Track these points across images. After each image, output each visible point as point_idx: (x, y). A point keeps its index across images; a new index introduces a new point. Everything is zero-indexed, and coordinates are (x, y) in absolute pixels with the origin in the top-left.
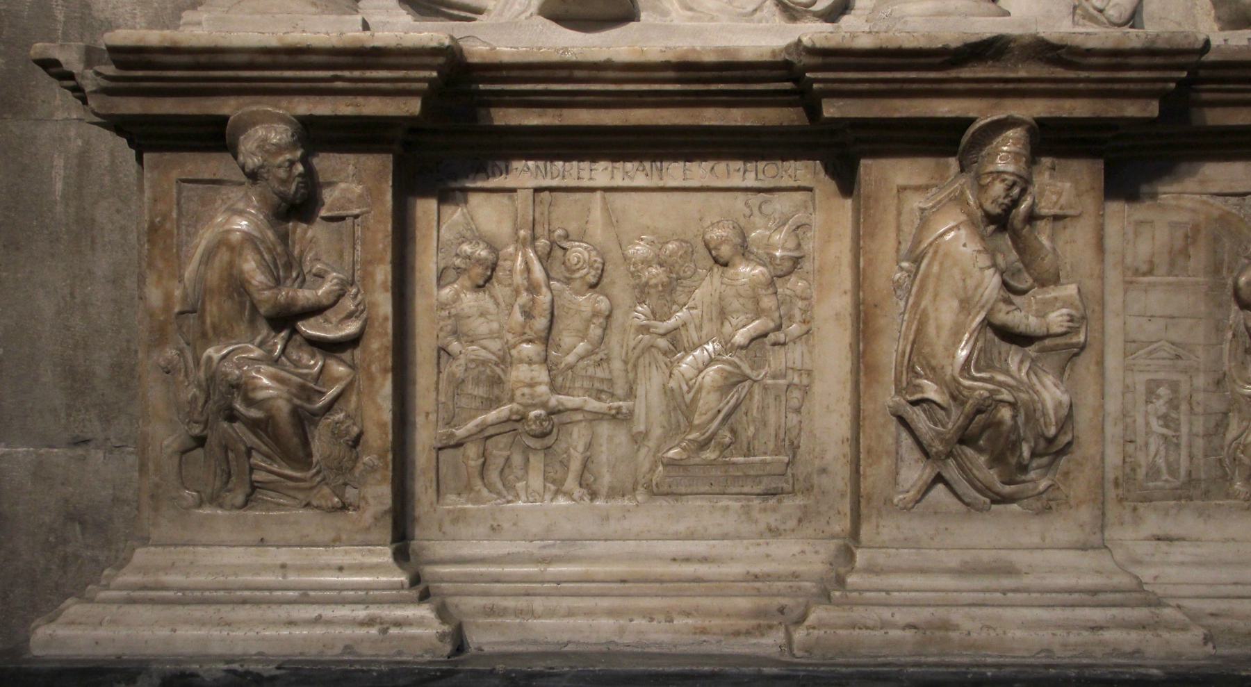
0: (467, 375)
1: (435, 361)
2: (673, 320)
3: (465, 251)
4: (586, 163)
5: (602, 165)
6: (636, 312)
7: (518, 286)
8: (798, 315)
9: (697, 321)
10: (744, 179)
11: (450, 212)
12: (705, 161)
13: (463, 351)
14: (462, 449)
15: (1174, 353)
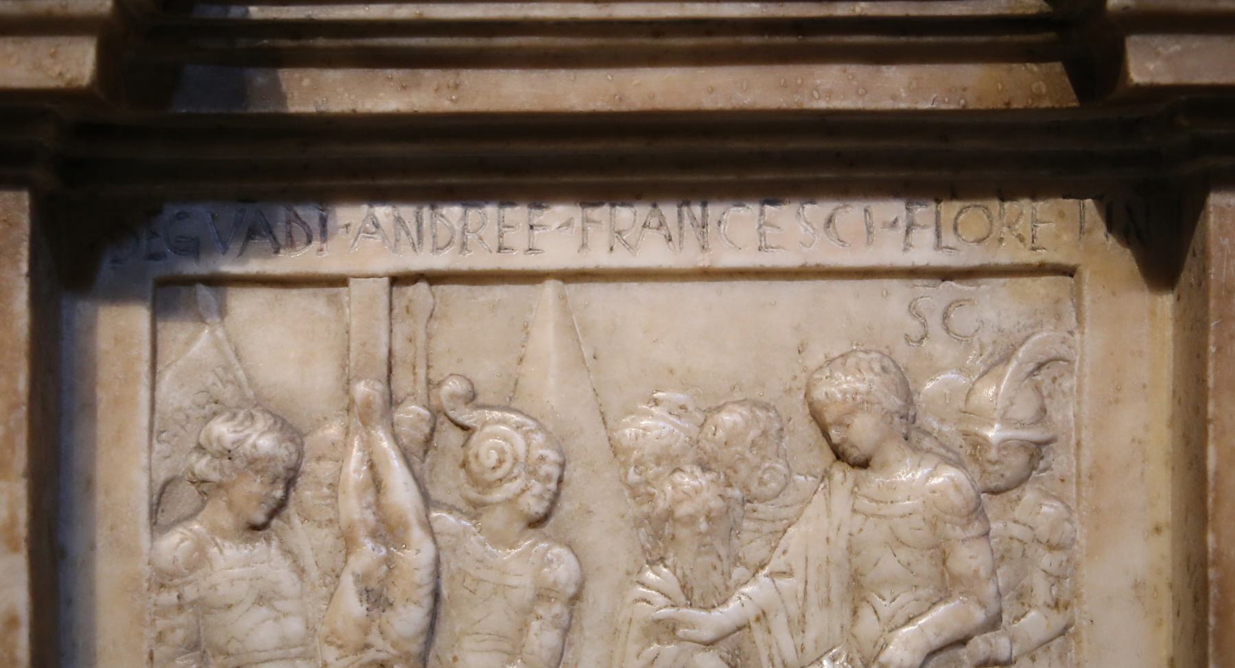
2: (733, 605)
3: (219, 440)
4: (517, 208)
5: (559, 213)
6: (643, 585)
7: (351, 527)
8: (1042, 590)
9: (794, 609)
10: (907, 247)
11: (182, 336)
12: (812, 202)
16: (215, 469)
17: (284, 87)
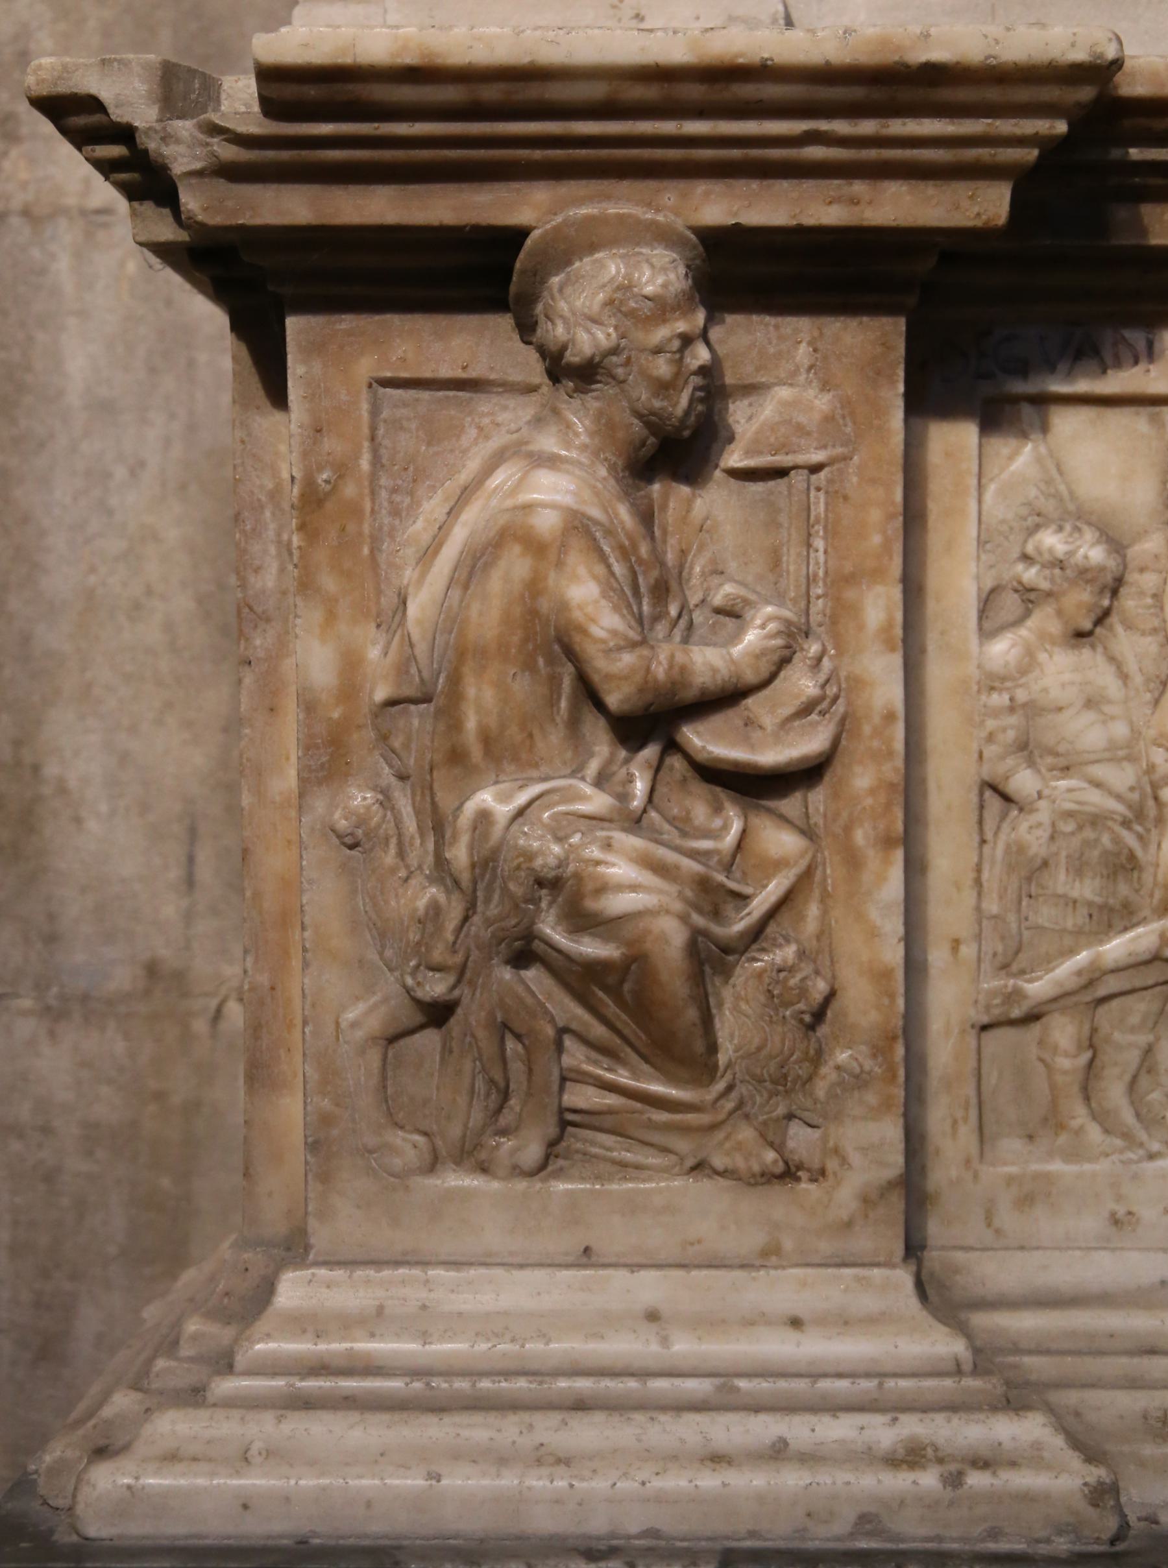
0: (1054, 849)
1: (974, 817)
13: (1046, 792)
14: (1036, 1029)
16: (1045, 578)
17: (1146, 221)
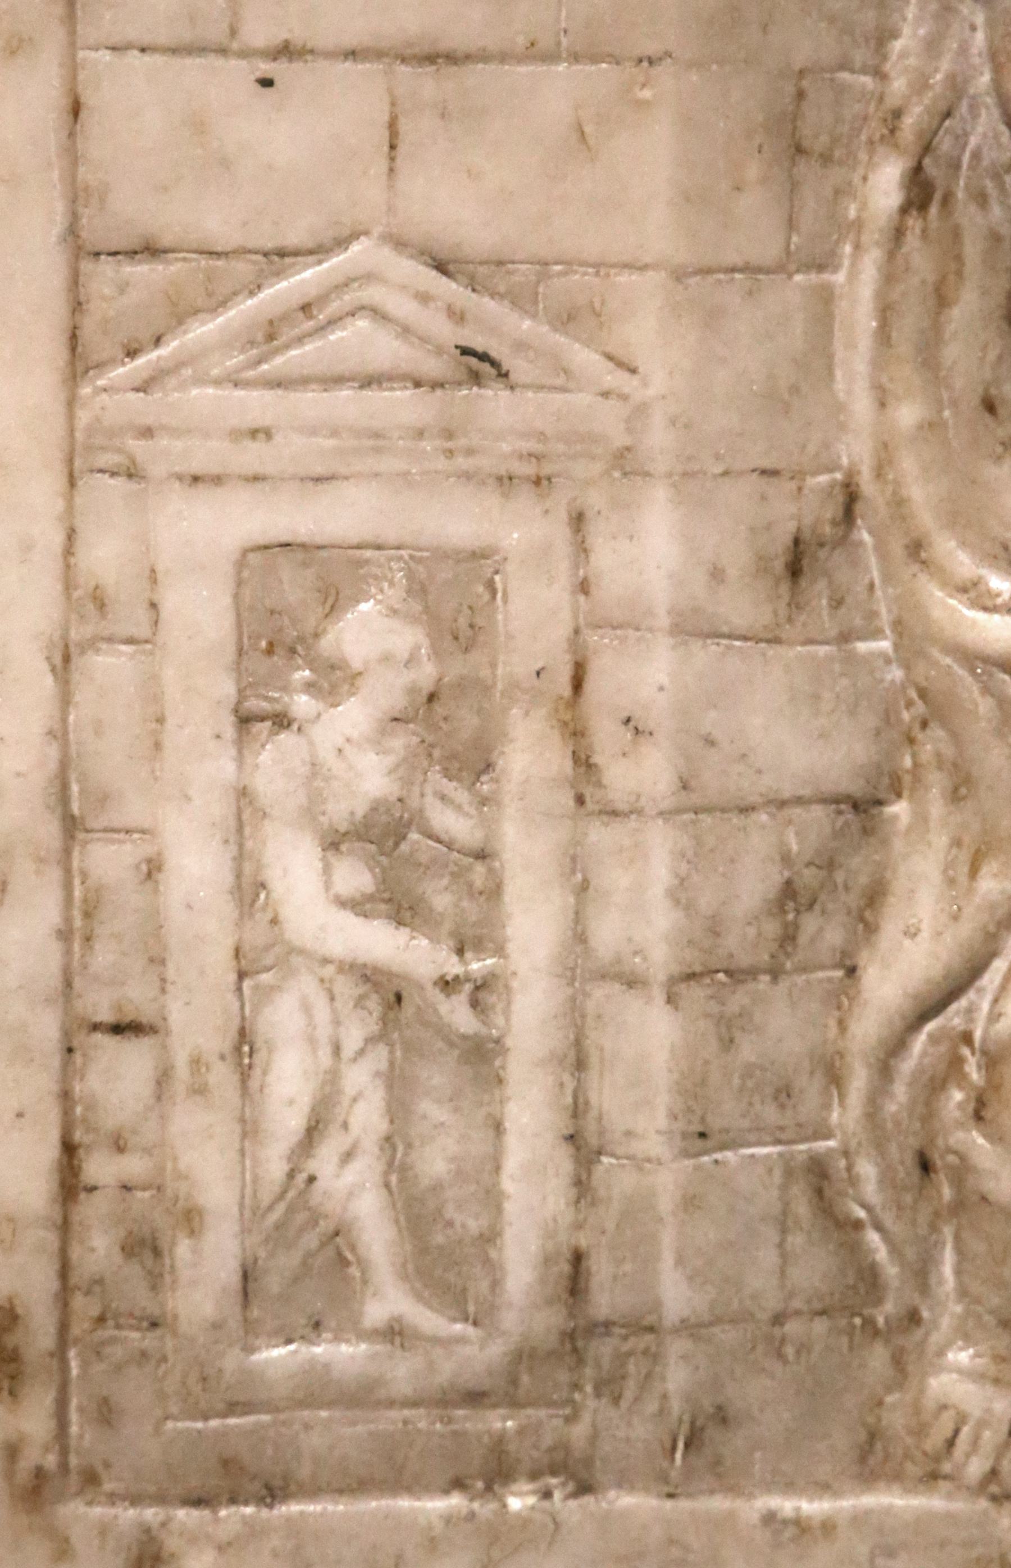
15: (449, 334)
